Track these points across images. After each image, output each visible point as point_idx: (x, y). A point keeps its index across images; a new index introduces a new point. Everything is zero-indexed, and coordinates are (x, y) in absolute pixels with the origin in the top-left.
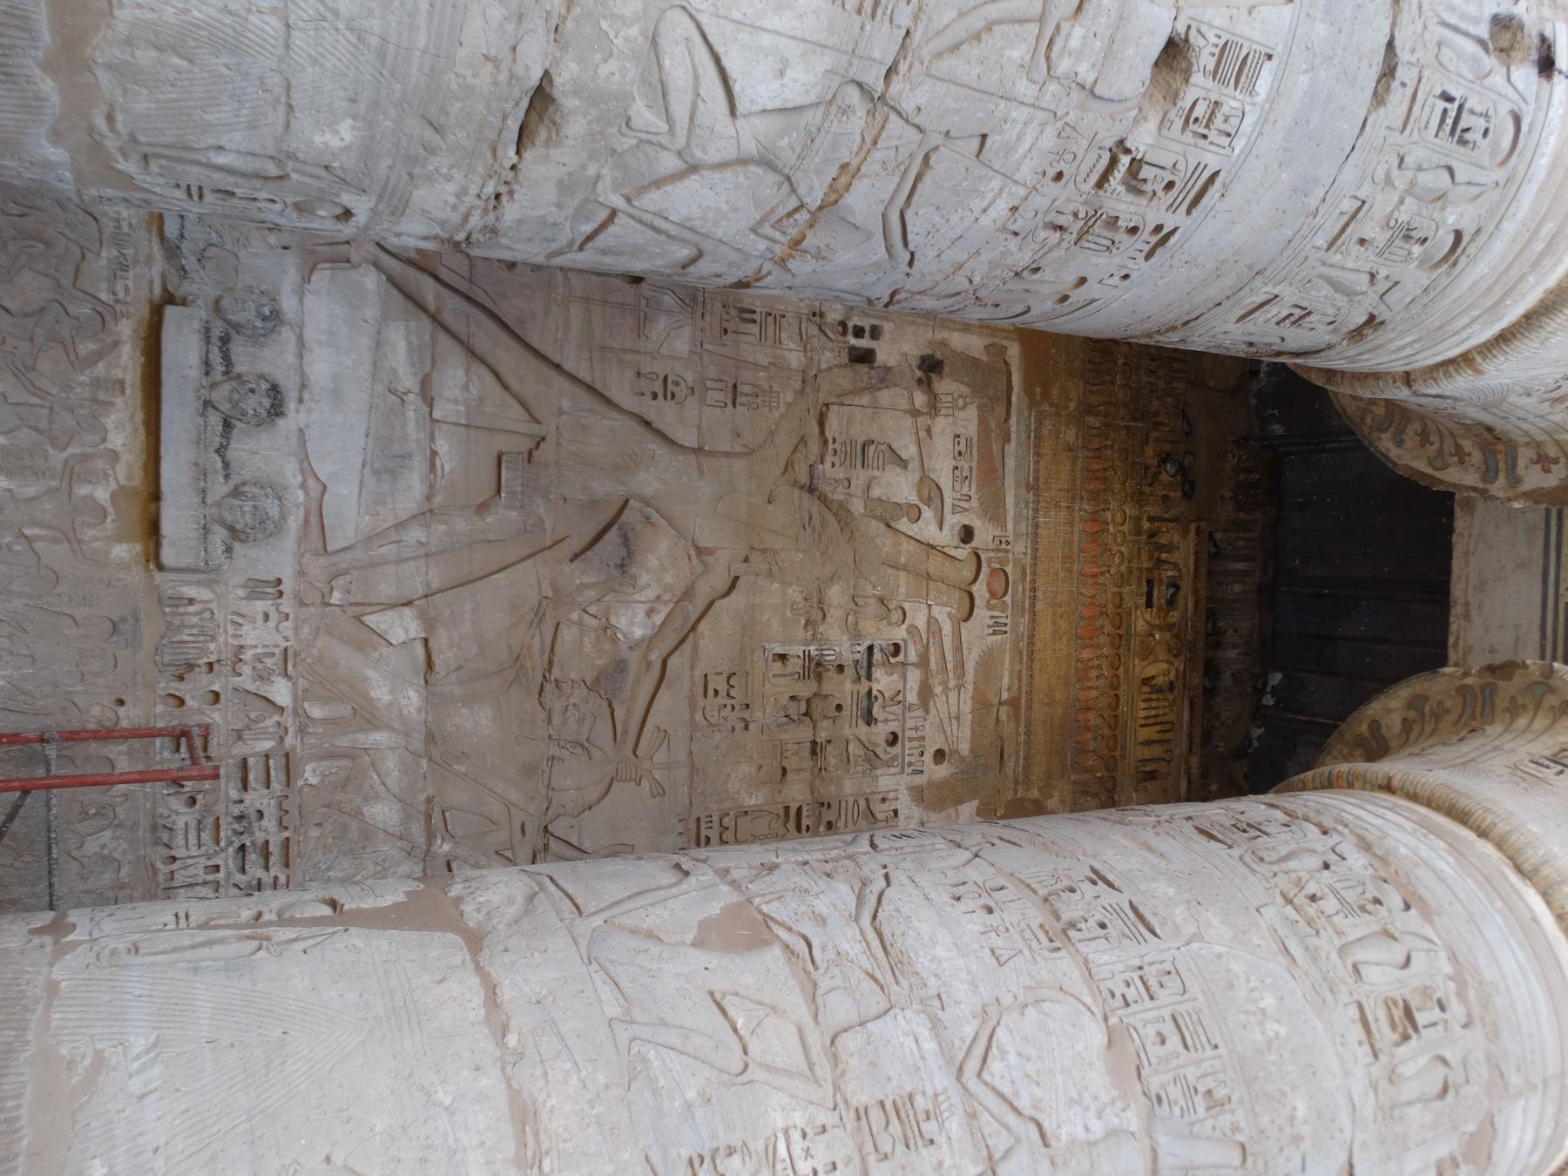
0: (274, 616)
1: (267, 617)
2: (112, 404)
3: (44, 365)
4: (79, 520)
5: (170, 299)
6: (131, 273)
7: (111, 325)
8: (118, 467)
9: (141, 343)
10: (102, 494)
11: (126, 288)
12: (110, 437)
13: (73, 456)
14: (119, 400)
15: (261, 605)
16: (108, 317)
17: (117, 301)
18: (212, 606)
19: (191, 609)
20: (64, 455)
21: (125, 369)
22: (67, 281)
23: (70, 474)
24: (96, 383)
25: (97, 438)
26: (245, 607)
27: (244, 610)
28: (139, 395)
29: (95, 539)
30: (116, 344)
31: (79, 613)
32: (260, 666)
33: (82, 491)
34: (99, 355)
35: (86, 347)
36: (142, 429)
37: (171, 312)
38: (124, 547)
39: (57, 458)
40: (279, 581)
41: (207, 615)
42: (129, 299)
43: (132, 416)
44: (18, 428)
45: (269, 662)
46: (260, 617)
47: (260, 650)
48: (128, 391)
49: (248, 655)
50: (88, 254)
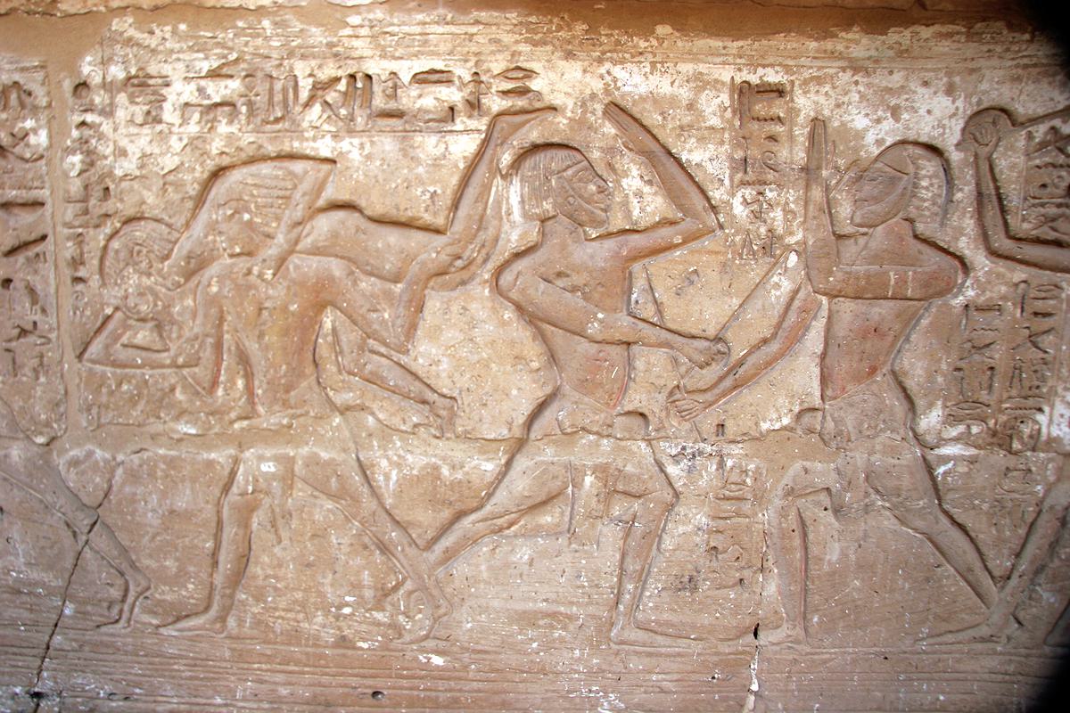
2: (818, 125)
3: (706, 310)
6: (375, 67)
9: (606, 36)
11: (422, 79)
12: (925, 129)
14: (805, 103)
16: (534, 134)
17: (474, 105)
20: (981, 261)
21: (701, 83)
22: (432, 250)
28: (784, 43)
30: (617, 110)
36: (899, 36)
42: (463, 72)
43: (856, 67)
48: (773, 76)
50: (330, 193)
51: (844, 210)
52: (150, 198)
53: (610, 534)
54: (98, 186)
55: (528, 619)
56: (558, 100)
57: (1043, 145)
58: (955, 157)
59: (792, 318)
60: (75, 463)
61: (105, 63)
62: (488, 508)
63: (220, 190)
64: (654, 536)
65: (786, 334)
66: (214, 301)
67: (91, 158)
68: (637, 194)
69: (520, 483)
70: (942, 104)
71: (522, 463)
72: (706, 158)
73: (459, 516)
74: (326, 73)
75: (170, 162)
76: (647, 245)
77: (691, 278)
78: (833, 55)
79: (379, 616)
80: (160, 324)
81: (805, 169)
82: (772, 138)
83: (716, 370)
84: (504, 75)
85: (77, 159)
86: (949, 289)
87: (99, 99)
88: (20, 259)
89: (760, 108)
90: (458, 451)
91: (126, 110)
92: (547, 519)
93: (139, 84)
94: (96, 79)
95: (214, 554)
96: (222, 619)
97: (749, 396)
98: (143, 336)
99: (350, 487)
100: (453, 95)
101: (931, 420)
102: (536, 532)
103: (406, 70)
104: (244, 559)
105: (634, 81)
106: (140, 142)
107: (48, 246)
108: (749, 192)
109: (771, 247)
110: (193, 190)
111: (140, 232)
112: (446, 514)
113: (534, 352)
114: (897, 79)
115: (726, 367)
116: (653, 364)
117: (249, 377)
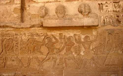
0: (107, 5)
1: (107, 6)
2: (64, 35)
3: (58, 47)
4: (88, 41)
5: (42, 26)
6: (38, 33)
7: (49, 36)
8: (77, 34)
9: (52, 31)
10: (83, 37)
11: (41, 34)
12: (71, 35)
13: (76, 42)
14: (64, 34)
15: (104, 7)
16: (47, 37)
17: (44, 35)
18: (105, 16)
19: (106, 20)
20: (75, 43)
21: (57, 33)
22: (42, 43)
23: (79, 42)
24: (61, 38)
25: (72, 38)
26: (105, 10)
27: (105, 10)
28: (62, 31)
29: (92, 38)
30: (52, 35)
31: (107, 40)
32: (117, 7)
33: (83, 40)
34: (55, 38)
35: (54, 40)
36: (69, 30)
37: (44, 26)
38: (93, 32)
39: (76, 44)
40: (99, 4)
41: (107, 17)
42: (43, 33)
43: (66, 32)
44: (71, 51)
45: (116, 5)
46: (107, 7)
47: (114, 7)
48: (62, 33)
49: (115, 10)
50: (36, 40)
51: (66, 40)
52: (25, 40)
53: (53, 61)
54: (22, 40)
55: (48, 67)
56: (48, 35)
57: (79, 36)
58: (73, 37)
59: (64, 47)
60: (19, 57)
61: (23, 32)
62: (45, 60)
63: (29, 40)
64: (56, 62)
65: (63, 48)
66: (29, 47)
67: (21, 38)
68: (54, 40)
69: (47, 58)
70: (72, 34)
71: (47, 56)
72: (57, 38)
73: (44, 60)
74: (36, 33)
75: (26, 38)
76: (54, 43)
77: (57, 45)
78: (65, 31)
79: (39, 67)
80: (25, 48)
81: (64, 38)
82: (62, 36)
83: (59, 50)
84: (46, 33)
85: (21, 38)
86: (74, 45)
87: (22, 35)
88: (17, 44)
89: (61, 35)
90: (43, 56)
91: (24, 35)
92: (49, 60)
93: (24, 34)
94: (22, 33)
95: (28, 63)
96: (28, 67)
97: (61, 52)
98: (24, 49)
99: (37, 58)
100: (42, 35)
101: (73, 53)
102: (49, 61)
103: (40, 33)
104: (30, 63)
105: (53, 33)
106: (24, 37)
107: (19, 43)
108: (60, 40)
109: (62, 43)
110: (27, 40)
111: (24, 42)
112: (43, 60)
113: (48, 50)
114: (69, 32)
115: (60, 50)
116: (55, 51)
117: (31, 51)
